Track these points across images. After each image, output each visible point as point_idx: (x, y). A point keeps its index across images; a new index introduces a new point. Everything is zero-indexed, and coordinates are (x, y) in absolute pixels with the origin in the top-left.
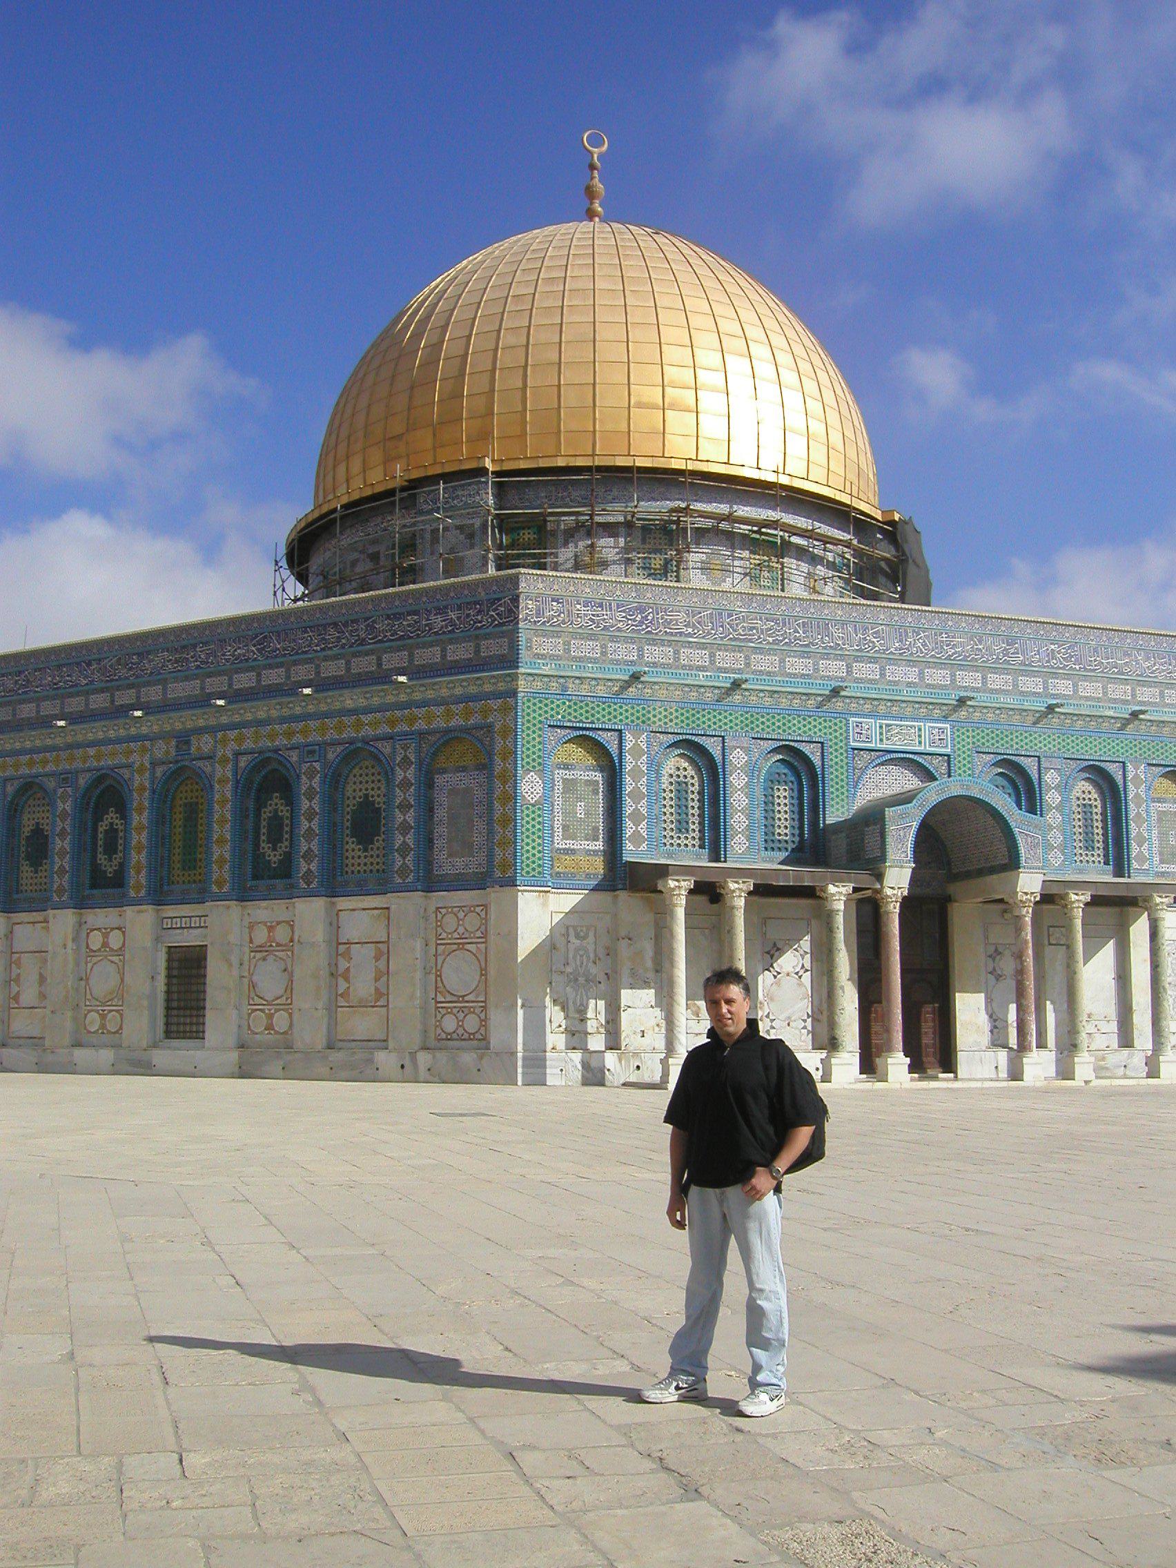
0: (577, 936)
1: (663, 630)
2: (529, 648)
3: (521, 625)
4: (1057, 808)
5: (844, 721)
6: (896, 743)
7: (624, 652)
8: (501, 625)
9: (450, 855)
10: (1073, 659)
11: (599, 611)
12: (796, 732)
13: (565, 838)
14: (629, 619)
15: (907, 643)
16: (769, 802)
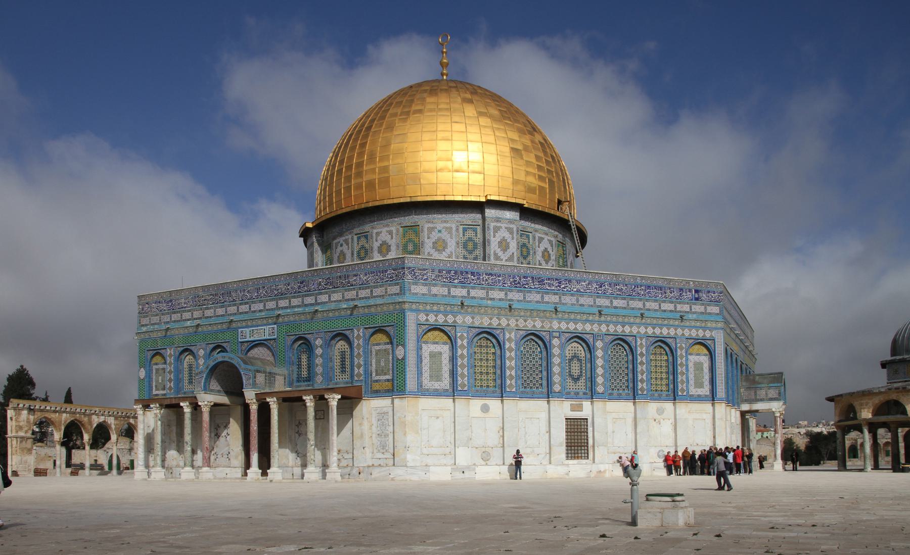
4: (321, 356)
7: (166, 318)
11: (159, 304)
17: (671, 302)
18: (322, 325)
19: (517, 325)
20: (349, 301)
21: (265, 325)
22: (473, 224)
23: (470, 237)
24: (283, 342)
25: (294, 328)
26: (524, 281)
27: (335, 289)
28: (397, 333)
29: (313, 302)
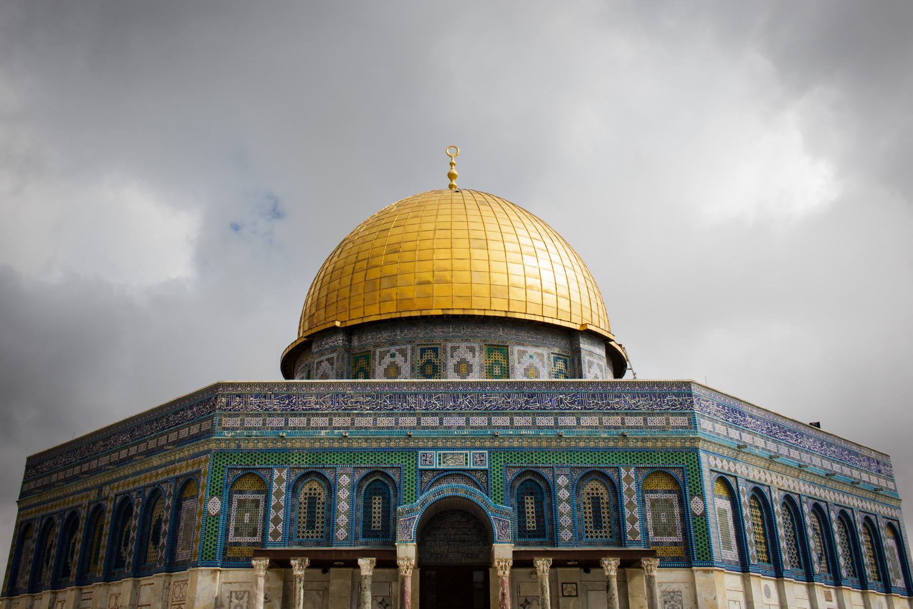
0: (237, 598)
1: (301, 408)
2: (220, 424)
3: (217, 412)
4: (567, 501)
5: (415, 454)
6: (451, 465)
7: (278, 422)
8: (210, 412)
9: (182, 549)
10: (576, 403)
11: (263, 400)
12: (384, 462)
13: (235, 536)
14: (280, 403)
15: (459, 402)
16: (368, 507)
17: (866, 472)
18: (567, 458)
19: (778, 483)
20: (609, 428)
21: (467, 449)
22: (564, 354)
23: (561, 368)
24: (500, 476)
25: (518, 457)
26: (775, 429)
27: (585, 411)
28: (689, 478)
29: (552, 423)
